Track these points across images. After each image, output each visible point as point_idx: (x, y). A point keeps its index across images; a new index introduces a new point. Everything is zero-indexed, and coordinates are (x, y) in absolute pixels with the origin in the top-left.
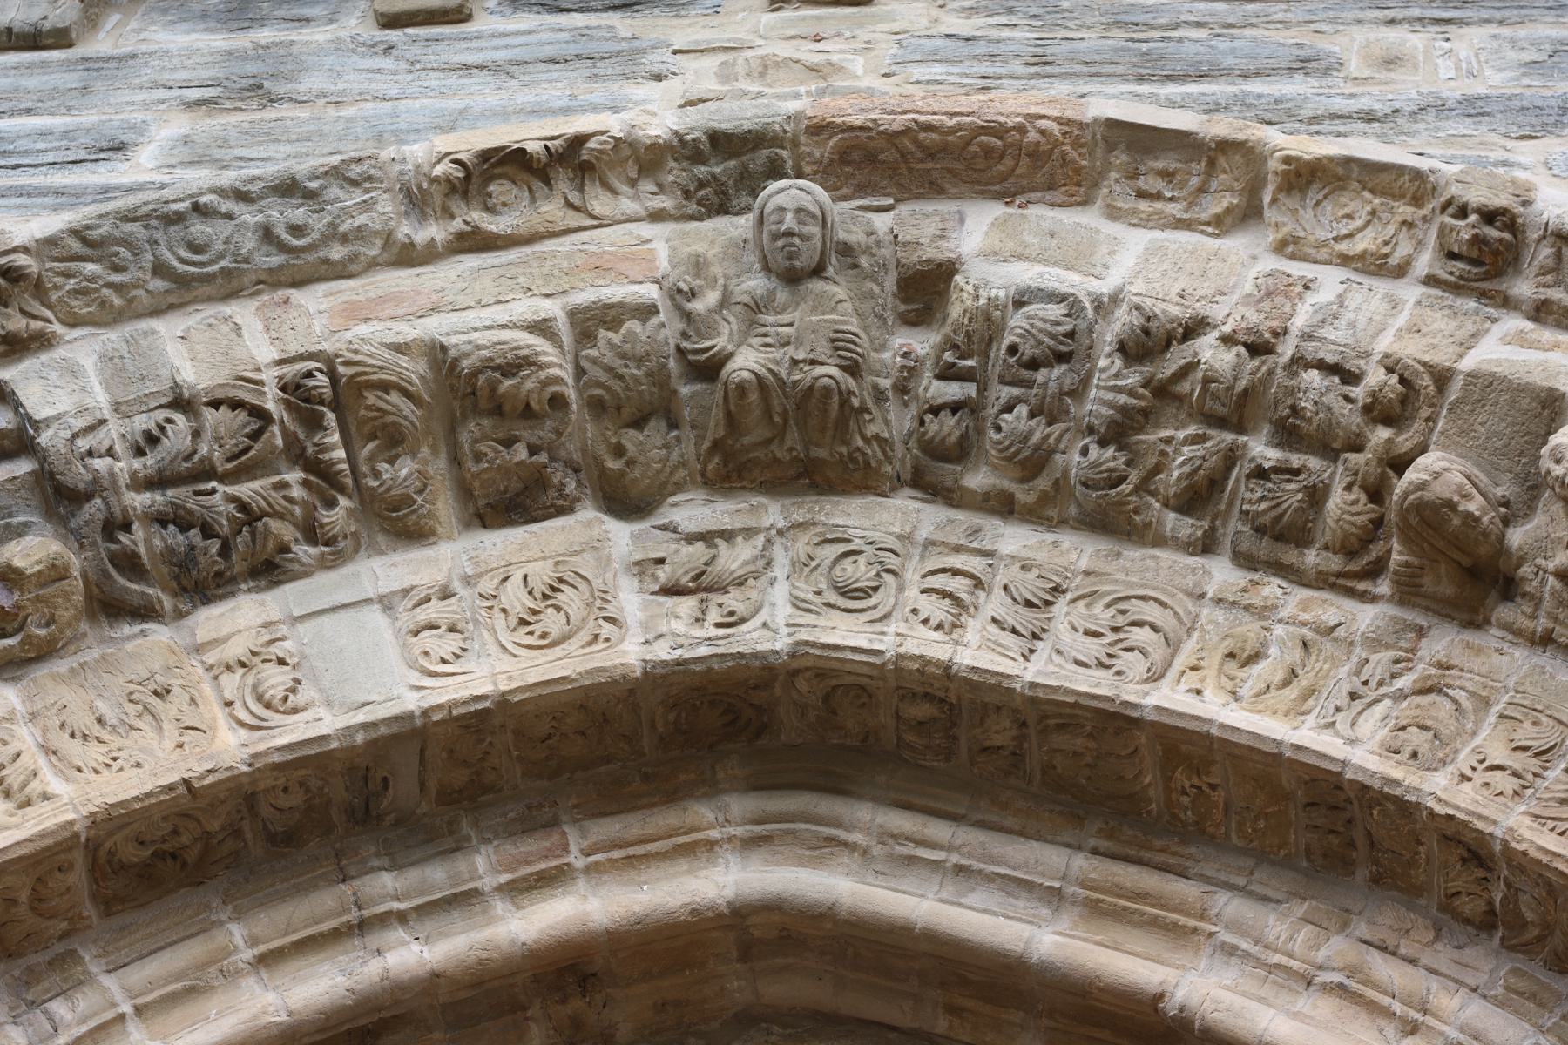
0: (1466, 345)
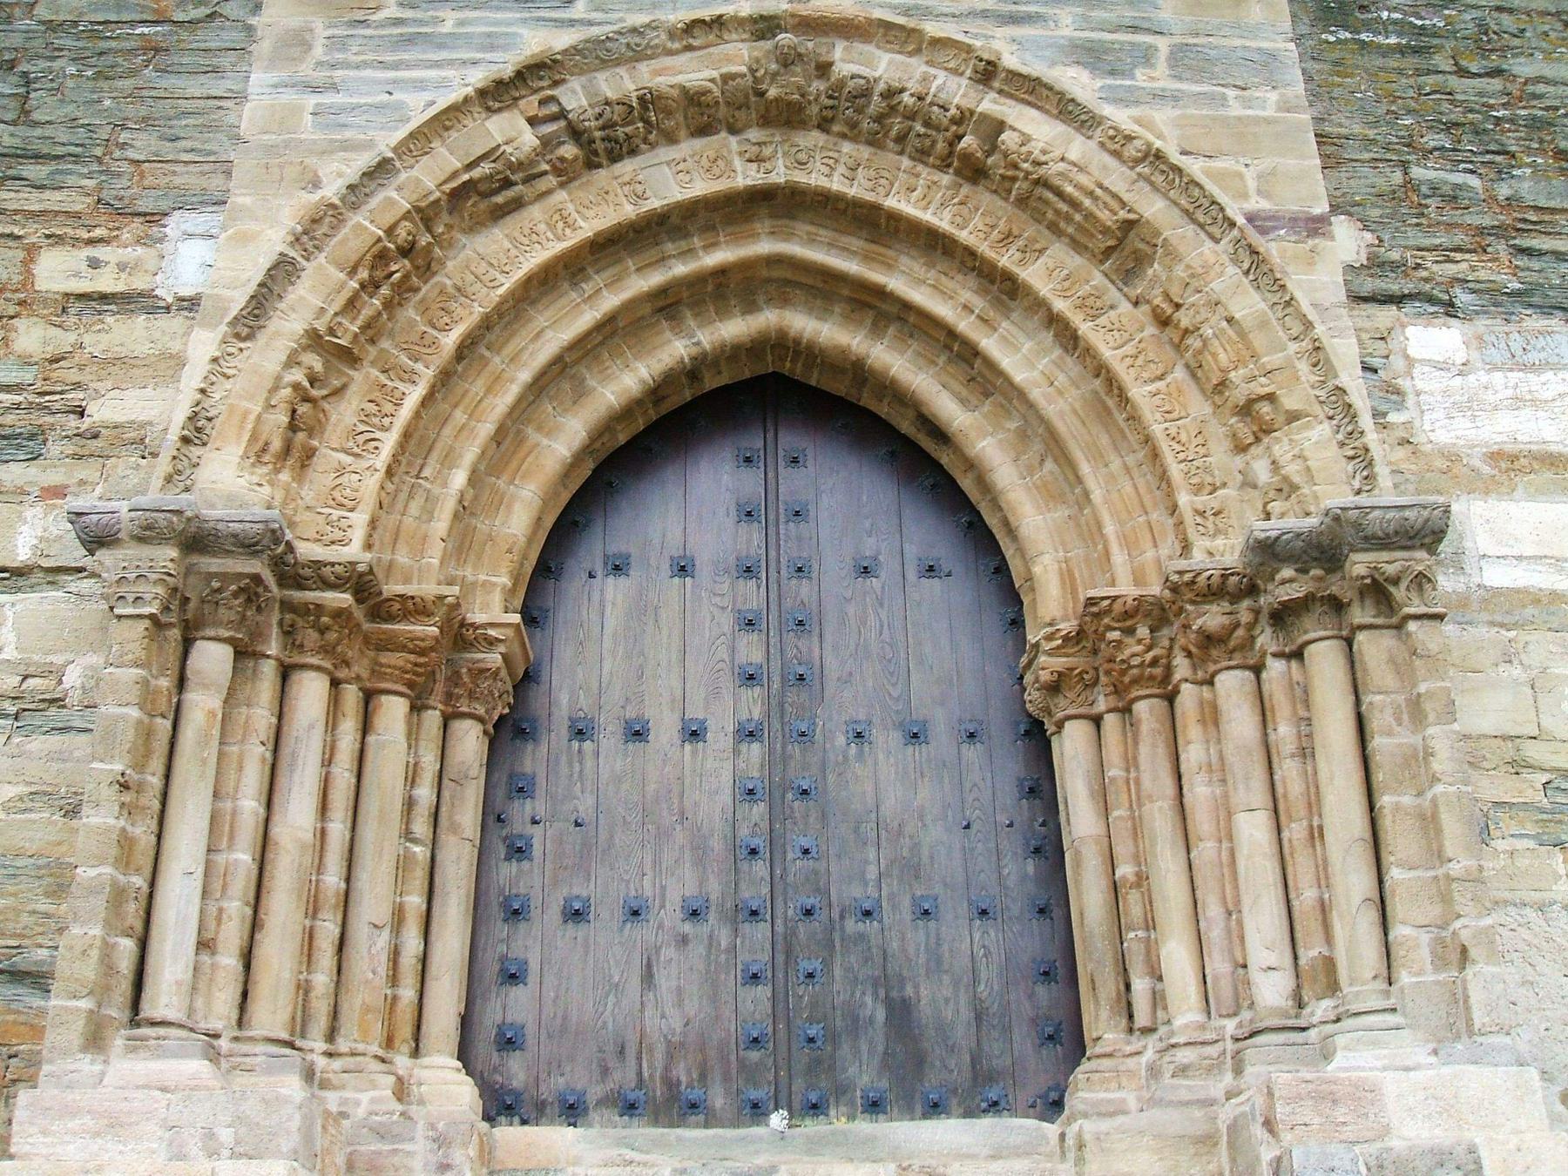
0: (980, 102)
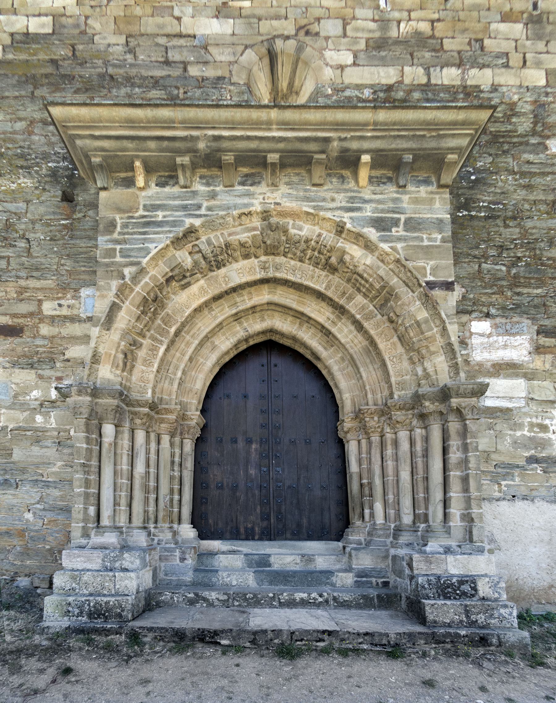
0: (337, 243)
